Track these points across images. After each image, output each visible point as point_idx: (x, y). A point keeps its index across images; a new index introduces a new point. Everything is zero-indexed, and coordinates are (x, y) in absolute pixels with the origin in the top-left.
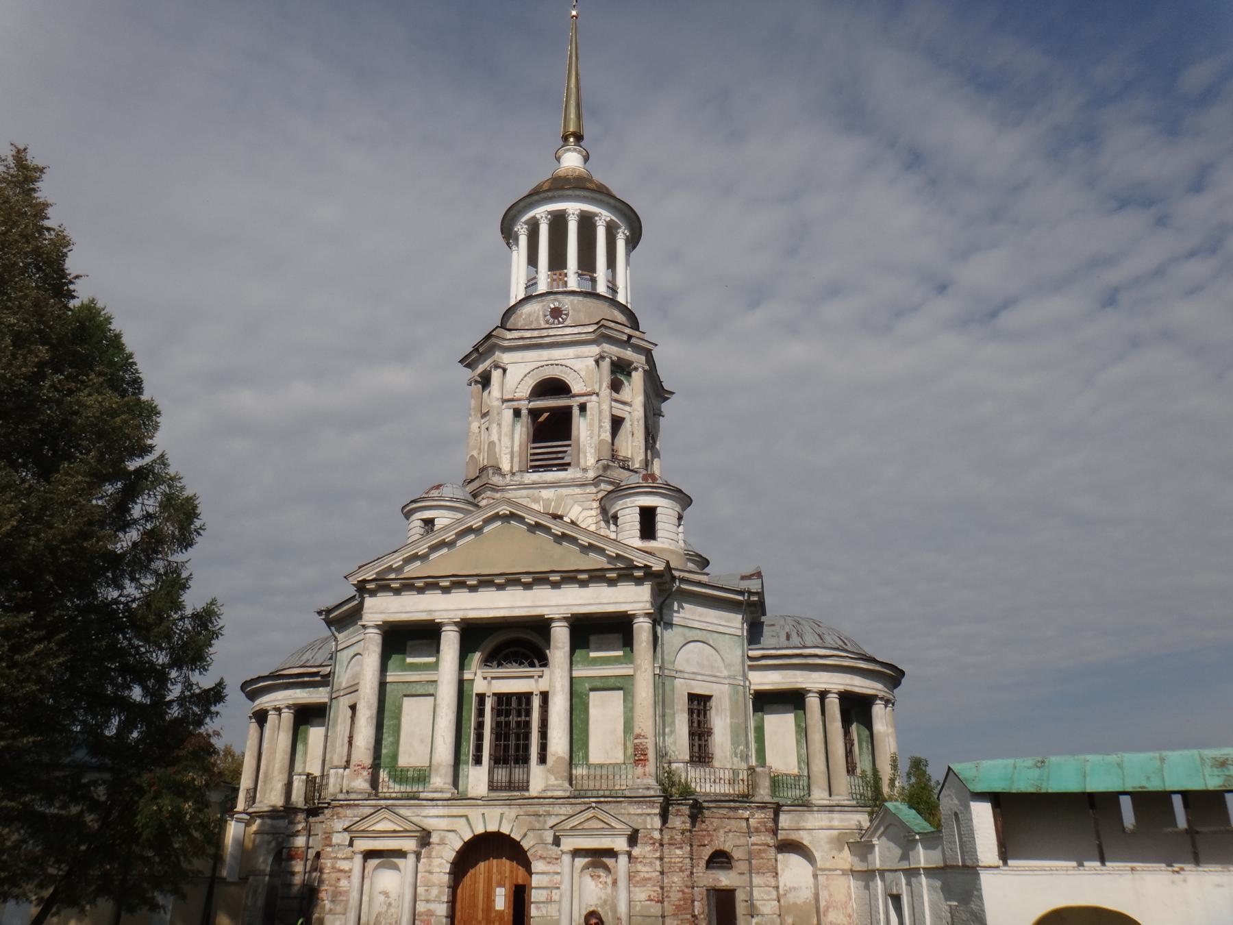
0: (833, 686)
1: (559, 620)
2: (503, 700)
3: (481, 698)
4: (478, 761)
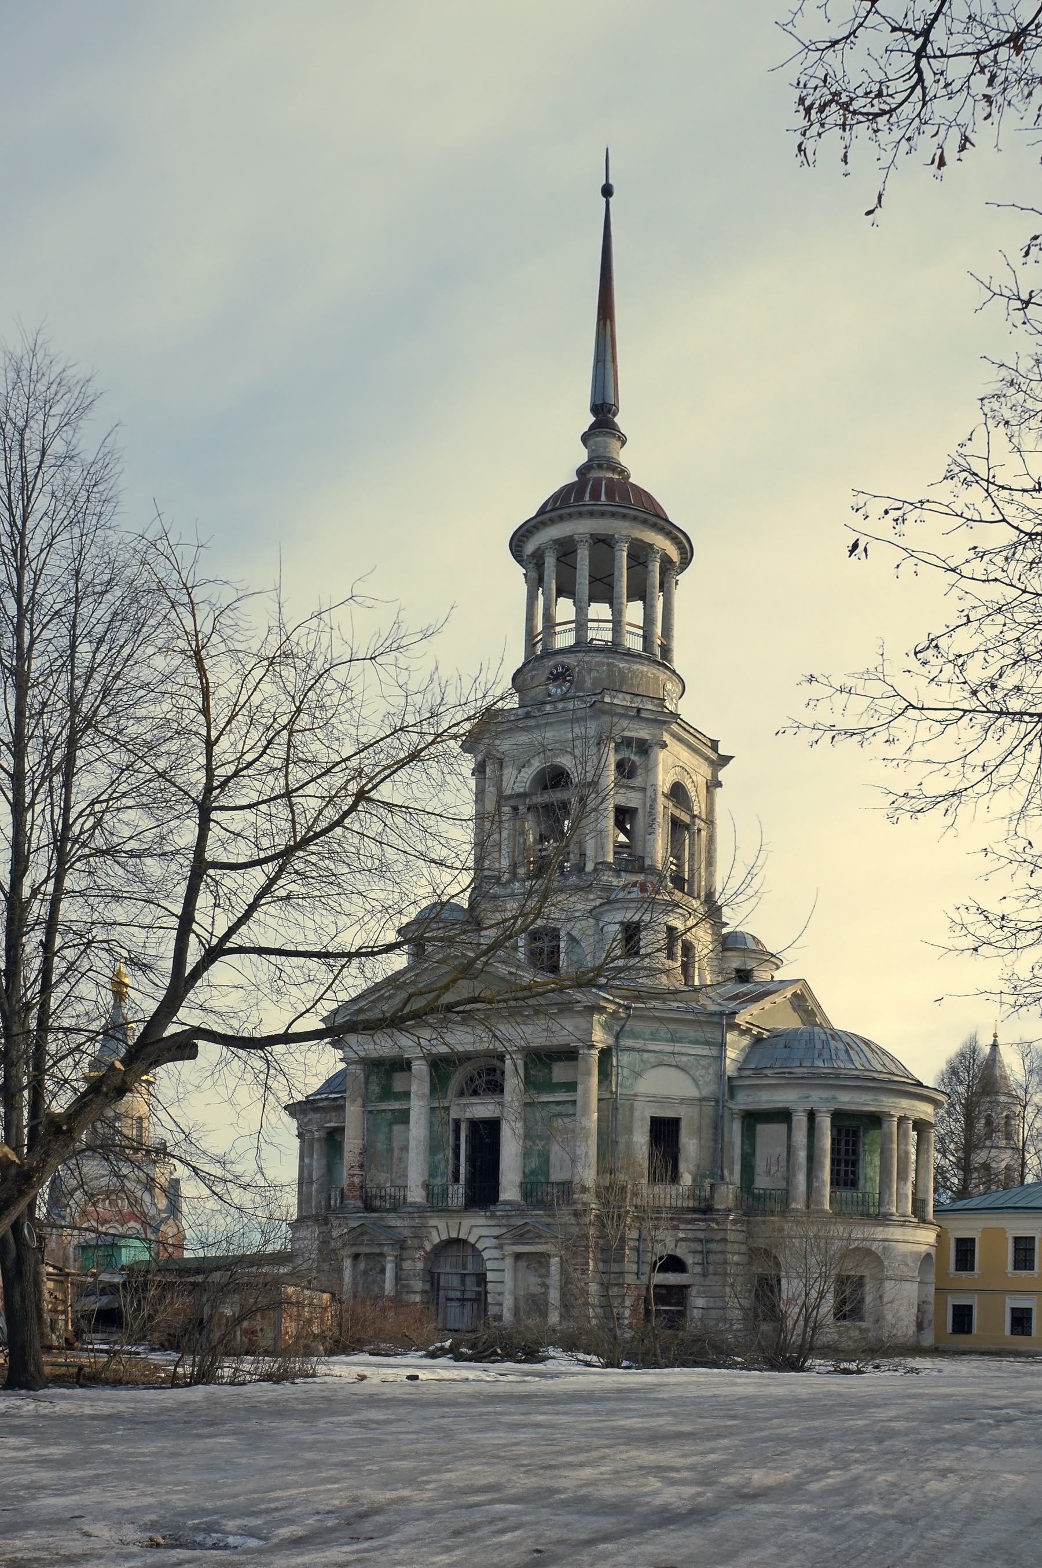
2: (475, 1124)
3: (457, 1123)
4: (456, 1180)
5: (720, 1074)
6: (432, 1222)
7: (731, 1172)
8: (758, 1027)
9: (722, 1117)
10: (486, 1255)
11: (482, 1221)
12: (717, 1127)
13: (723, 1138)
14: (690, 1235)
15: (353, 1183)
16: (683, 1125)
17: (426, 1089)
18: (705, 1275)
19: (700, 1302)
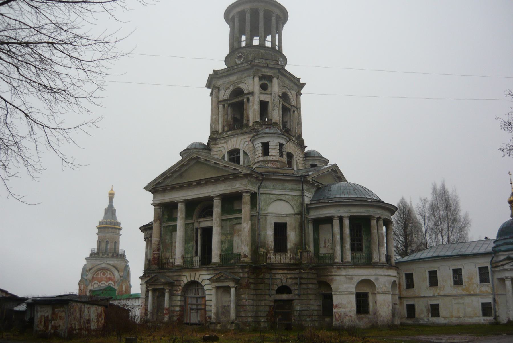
1: (217, 196)
3: (197, 229)
4: (196, 255)
5: (302, 203)
6: (184, 274)
7: (309, 247)
8: (317, 182)
10: (206, 288)
11: (204, 273)
12: (302, 228)
14: (292, 276)
16: (288, 226)
17: (184, 215)
18: (299, 295)
19: (298, 308)
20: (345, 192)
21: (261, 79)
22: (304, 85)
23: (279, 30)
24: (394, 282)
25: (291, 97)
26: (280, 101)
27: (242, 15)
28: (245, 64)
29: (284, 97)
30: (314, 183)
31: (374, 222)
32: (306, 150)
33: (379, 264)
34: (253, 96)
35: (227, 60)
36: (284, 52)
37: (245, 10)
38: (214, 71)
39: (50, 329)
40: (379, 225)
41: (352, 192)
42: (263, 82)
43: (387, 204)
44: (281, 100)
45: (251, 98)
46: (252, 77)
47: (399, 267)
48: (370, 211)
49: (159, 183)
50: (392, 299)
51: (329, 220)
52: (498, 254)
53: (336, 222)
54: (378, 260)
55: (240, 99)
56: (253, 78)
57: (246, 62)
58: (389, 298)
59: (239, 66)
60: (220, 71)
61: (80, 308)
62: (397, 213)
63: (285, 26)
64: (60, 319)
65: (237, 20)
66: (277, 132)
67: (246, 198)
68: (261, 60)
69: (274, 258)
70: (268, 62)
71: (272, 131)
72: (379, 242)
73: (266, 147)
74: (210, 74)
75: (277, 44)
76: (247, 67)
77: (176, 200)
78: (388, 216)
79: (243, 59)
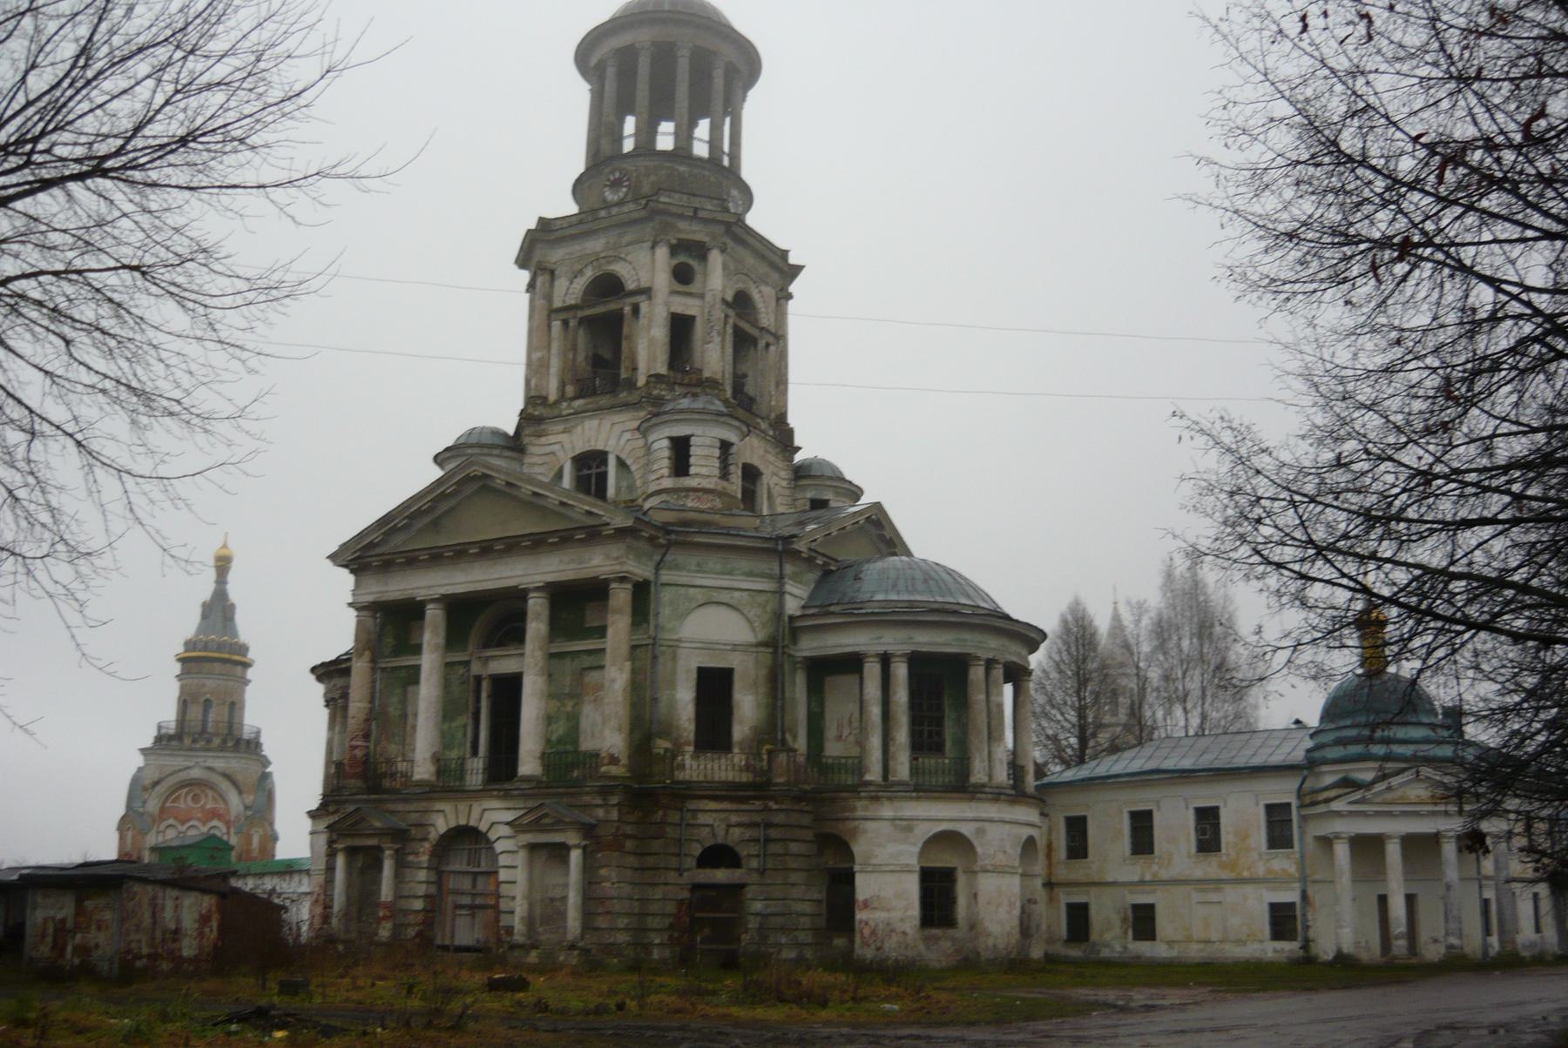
0: (896, 647)
1: (537, 589)
3: (478, 679)
4: (475, 752)
5: (778, 614)
7: (795, 737)
8: (823, 555)
9: (782, 666)
12: (775, 683)
13: (783, 692)
14: (745, 819)
15: (355, 756)
16: (737, 677)
18: (762, 872)
19: (758, 906)
20: (901, 584)
21: (674, 250)
22: (798, 269)
23: (732, 107)
24: (1030, 843)
25: (760, 305)
26: (727, 316)
27: (627, 57)
28: (632, 206)
29: (741, 303)
30: (815, 558)
31: (977, 673)
32: (798, 457)
33: (987, 790)
34: (650, 298)
35: (579, 188)
36: (748, 173)
37: (637, 45)
38: (541, 219)
39: (68, 956)
40: (991, 679)
41: (920, 587)
42: (682, 258)
43: (1017, 621)
44: (731, 312)
45: (644, 307)
46: (648, 244)
47: (1045, 798)
48: (966, 640)
49: (371, 545)
50: (1023, 887)
51: (852, 663)
52: (1317, 770)
53: (872, 670)
54: (985, 779)
55: (613, 306)
56: (653, 247)
57: (635, 200)
58: (1012, 884)
59: (614, 211)
60: (559, 222)
61: (154, 898)
62: (1043, 647)
63: (752, 94)
64: (99, 929)
65: (611, 72)
66: (713, 408)
67: (621, 597)
68: (677, 196)
69: (694, 768)
70: (696, 202)
71: (699, 404)
72: (989, 727)
73: (681, 448)
74: (529, 231)
75: (726, 148)
76: (635, 215)
77: (421, 595)
78: (1019, 655)
79: (624, 190)
